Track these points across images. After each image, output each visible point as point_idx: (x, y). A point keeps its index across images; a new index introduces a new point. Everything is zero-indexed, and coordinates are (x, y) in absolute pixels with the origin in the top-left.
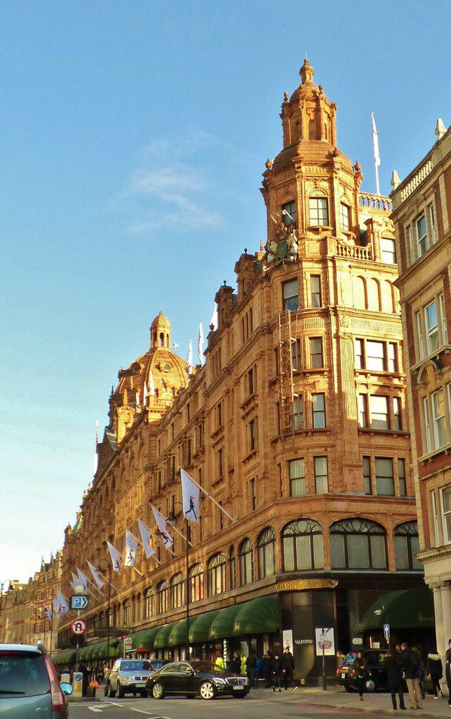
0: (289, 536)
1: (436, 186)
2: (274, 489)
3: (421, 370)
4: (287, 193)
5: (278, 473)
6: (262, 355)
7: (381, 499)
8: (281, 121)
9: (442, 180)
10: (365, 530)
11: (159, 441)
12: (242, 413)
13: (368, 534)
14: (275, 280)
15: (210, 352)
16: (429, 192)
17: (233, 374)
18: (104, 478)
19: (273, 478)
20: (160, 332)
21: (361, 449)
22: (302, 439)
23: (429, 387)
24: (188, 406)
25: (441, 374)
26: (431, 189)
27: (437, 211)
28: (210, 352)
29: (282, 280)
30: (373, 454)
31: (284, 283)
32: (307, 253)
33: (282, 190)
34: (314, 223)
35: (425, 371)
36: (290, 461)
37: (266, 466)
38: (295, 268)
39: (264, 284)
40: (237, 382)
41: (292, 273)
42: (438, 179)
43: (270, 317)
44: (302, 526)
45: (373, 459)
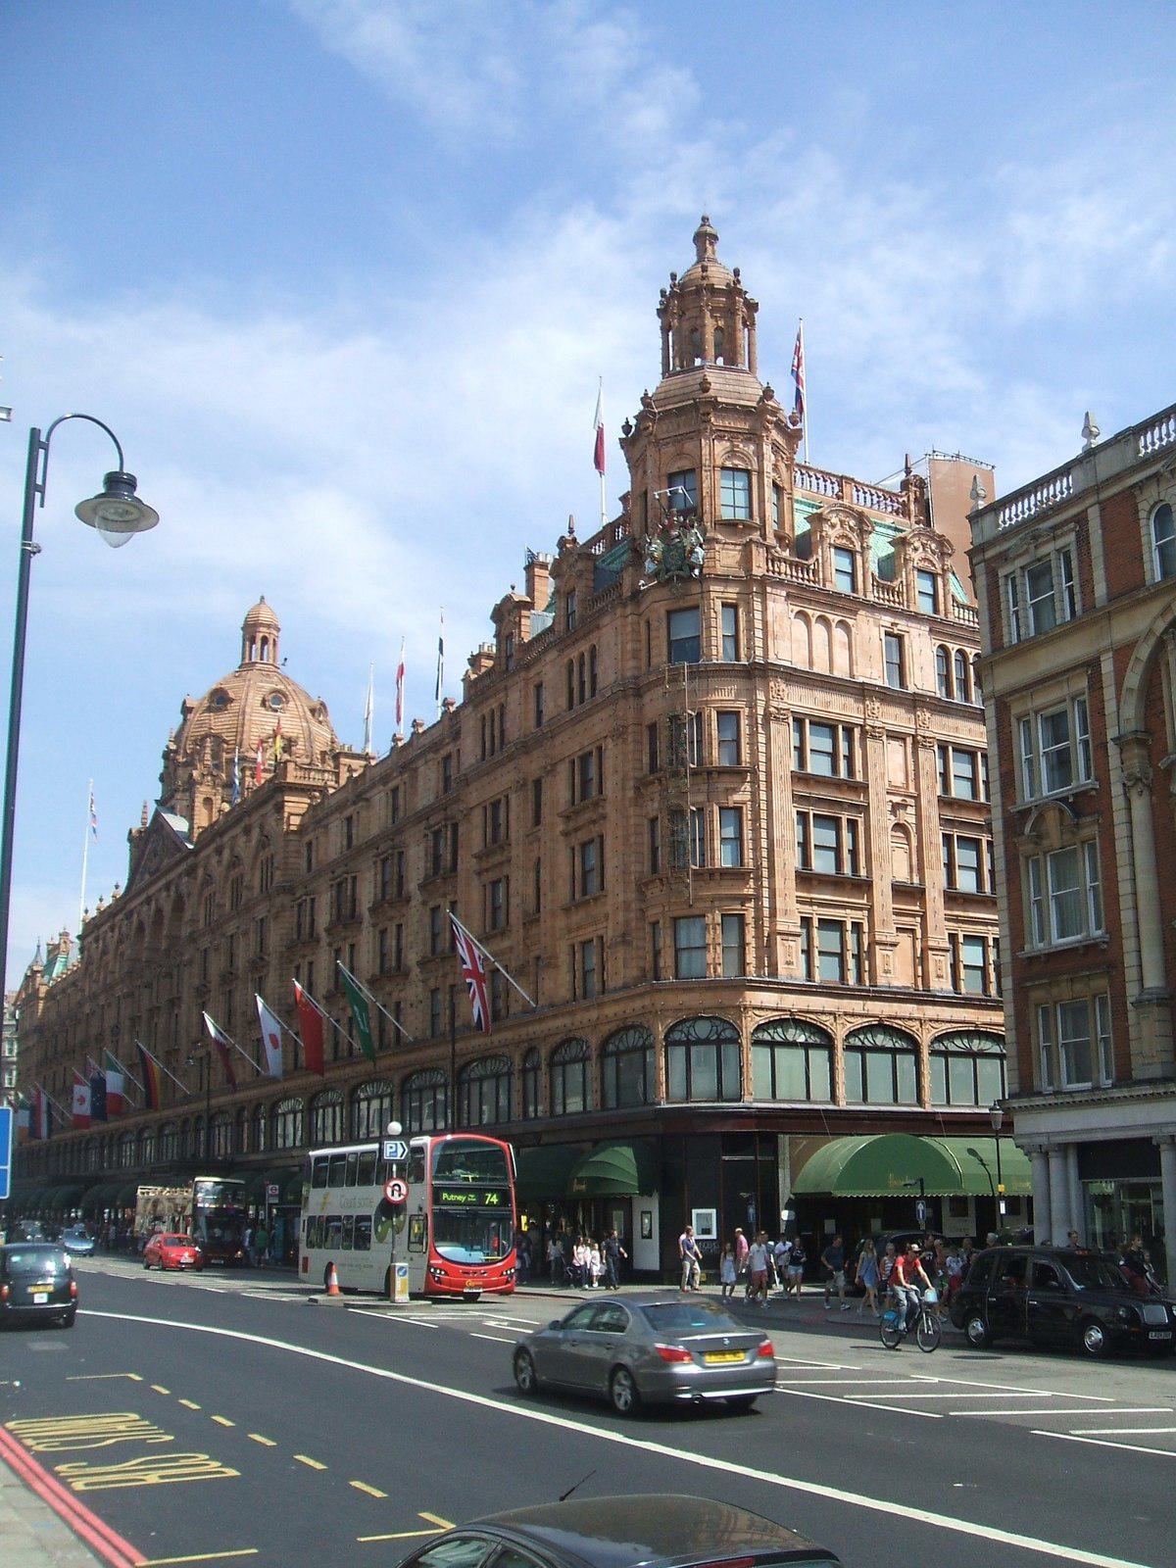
1: (1081, 520)
2: (641, 964)
3: (1034, 816)
4: (680, 454)
5: (648, 937)
6: (619, 734)
7: (826, 991)
8: (658, 322)
9: (1094, 515)
11: (309, 844)
12: (561, 828)
13: (806, 1046)
14: (656, 605)
15: (476, 707)
16: (1066, 529)
17: (535, 753)
18: (152, 890)
19: (640, 944)
20: (261, 635)
21: (799, 906)
22: (702, 883)
23: (1046, 843)
24: (395, 791)
25: (1077, 826)
26: (1072, 525)
27: (1080, 561)
28: (476, 707)
30: (816, 913)
31: (669, 613)
32: (718, 565)
33: (670, 449)
34: (727, 514)
35: (1041, 816)
36: (675, 920)
37: (627, 923)
38: (696, 589)
39: (629, 610)
40: (551, 770)
41: (687, 598)
42: (1085, 511)
43: (638, 668)
44: (702, 1029)
45: (816, 923)
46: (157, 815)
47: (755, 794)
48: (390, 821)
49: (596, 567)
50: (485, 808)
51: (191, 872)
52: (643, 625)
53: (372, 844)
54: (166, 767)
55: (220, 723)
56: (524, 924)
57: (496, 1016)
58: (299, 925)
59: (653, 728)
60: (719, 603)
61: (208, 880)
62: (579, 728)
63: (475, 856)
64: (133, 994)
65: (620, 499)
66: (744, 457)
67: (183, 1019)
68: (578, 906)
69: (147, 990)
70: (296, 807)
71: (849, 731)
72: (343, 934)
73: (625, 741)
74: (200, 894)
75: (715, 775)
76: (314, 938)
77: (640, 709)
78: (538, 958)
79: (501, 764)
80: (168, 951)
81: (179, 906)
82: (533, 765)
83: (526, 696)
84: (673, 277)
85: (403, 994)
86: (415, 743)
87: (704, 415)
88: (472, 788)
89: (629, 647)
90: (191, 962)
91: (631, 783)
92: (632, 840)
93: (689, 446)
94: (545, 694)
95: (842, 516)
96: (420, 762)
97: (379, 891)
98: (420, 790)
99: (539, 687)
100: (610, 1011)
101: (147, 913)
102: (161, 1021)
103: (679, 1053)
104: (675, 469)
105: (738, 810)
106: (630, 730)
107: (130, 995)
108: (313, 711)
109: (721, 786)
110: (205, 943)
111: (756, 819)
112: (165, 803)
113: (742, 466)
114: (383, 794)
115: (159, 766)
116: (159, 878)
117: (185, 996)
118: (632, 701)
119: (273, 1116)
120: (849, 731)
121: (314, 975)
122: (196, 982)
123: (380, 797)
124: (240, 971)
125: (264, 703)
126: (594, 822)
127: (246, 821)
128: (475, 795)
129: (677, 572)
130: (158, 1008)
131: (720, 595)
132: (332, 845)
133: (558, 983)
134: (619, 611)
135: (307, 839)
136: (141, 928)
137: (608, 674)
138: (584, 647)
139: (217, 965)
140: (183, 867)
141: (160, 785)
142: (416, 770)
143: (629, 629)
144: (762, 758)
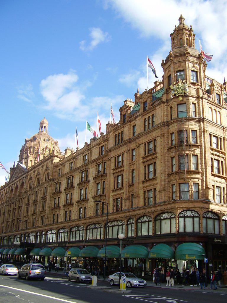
0: (181, 217)
2: (169, 196)
4: (180, 66)
10: (213, 217)
14: (174, 103)
17: (133, 143)
18: (15, 182)
19: (168, 190)
22: (188, 174)
29: (177, 103)
30: (216, 184)
31: (178, 105)
33: (177, 65)
36: (180, 184)
37: (165, 184)
38: (185, 99)
39: (165, 104)
40: (138, 147)
44: (189, 213)
46: (18, 164)
47: (201, 152)
48: (84, 163)
49: (152, 96)
50: (116, 157)
51: (26, 177)
52: (169, 109)
53: (78, 168)
54: (21, 154)
55: (33, 144)
56: (129, 186)
57: (117, 210)
58: (56, 188)
59: (172, 134)
60: (191, 104)
61: (31, 179)
62: (148, 135)
63: (112, 169)
64: (9, 205)
65: (154, 83)
66: (196, 68)
67: (22, 211)
68: (147, 181)
69: (13, 204)
70: (56, 160)
71: (220, 138)
72: (69, 190)
73: (164, 137)
74: (28, 182)
75: (191, 146)
76: (60, 192)
77: (168, 129)
78: (132, 195)
79: (122, 146)
80: (19, 195)
81: (23, 184)
82: (133, 145)
83: (130, 128)
84: (175, 26)
85: (87, 205)
86: (92, 144)
87: (187, 56)
88: (112, 153)
89: (165, 113)
90: (25, 198)
91: (166, 148)
92: (166, 163)
93: (182, 64)
94: (136, 128)
95: (217, 86)
96: (93, 148)
97: (81, 179)
98: (93, 155)
99: (134, 126)
100: (159, 208)
101: (14, 187)
102: (17, 211)
103: (182, 220)
104: (178, 70)
105: (197, 156)
106: (166, 134)
107: (8, 205)
108: (55, 143)
109: (193, 149)
110: (29, 193)
111: (201, 159)
112: (20, 161)
113: (195, 70)
114: (82, 157)
115: (19, 153)
116: (18, 179)
117: (23, 206)
118: (166, 127)
119: (46, 234)
120: (220, 138)
121: (59, 201)
122: (26, 202)
123: (81, 158)
124: (38, 200)
125: (44, 140)
126: (153, 159)
127: (42, 164)
128: (112, 154)
129: (181, 94)
130: (16, 208)
131: (192, 100)
132: (67, 169)
133: (140, 202)
134: (162, 105)
135: (59, 168)
136: (12, 190)
137: (158, 120)
138: (150, 115)
139: (32, 198)
140: (24, 176)
141: (19, 158)
142: (92, 150)
143: (165, 109)
144: (203, 143)
